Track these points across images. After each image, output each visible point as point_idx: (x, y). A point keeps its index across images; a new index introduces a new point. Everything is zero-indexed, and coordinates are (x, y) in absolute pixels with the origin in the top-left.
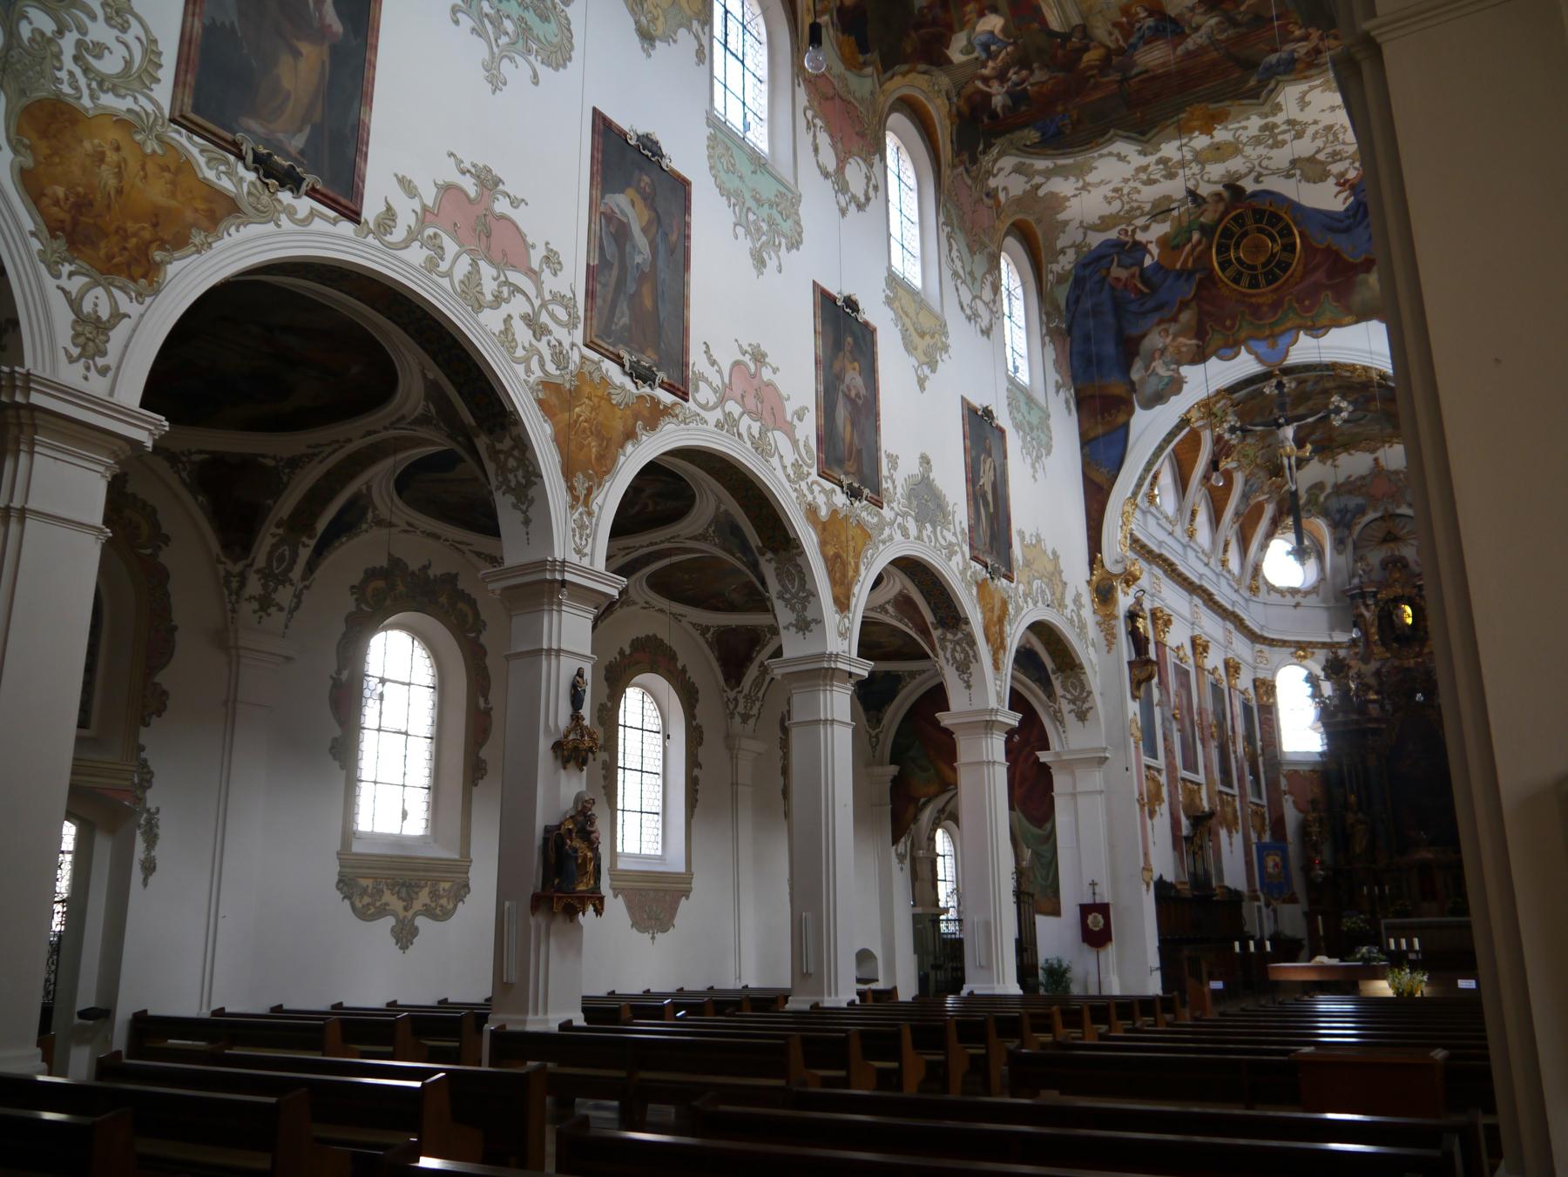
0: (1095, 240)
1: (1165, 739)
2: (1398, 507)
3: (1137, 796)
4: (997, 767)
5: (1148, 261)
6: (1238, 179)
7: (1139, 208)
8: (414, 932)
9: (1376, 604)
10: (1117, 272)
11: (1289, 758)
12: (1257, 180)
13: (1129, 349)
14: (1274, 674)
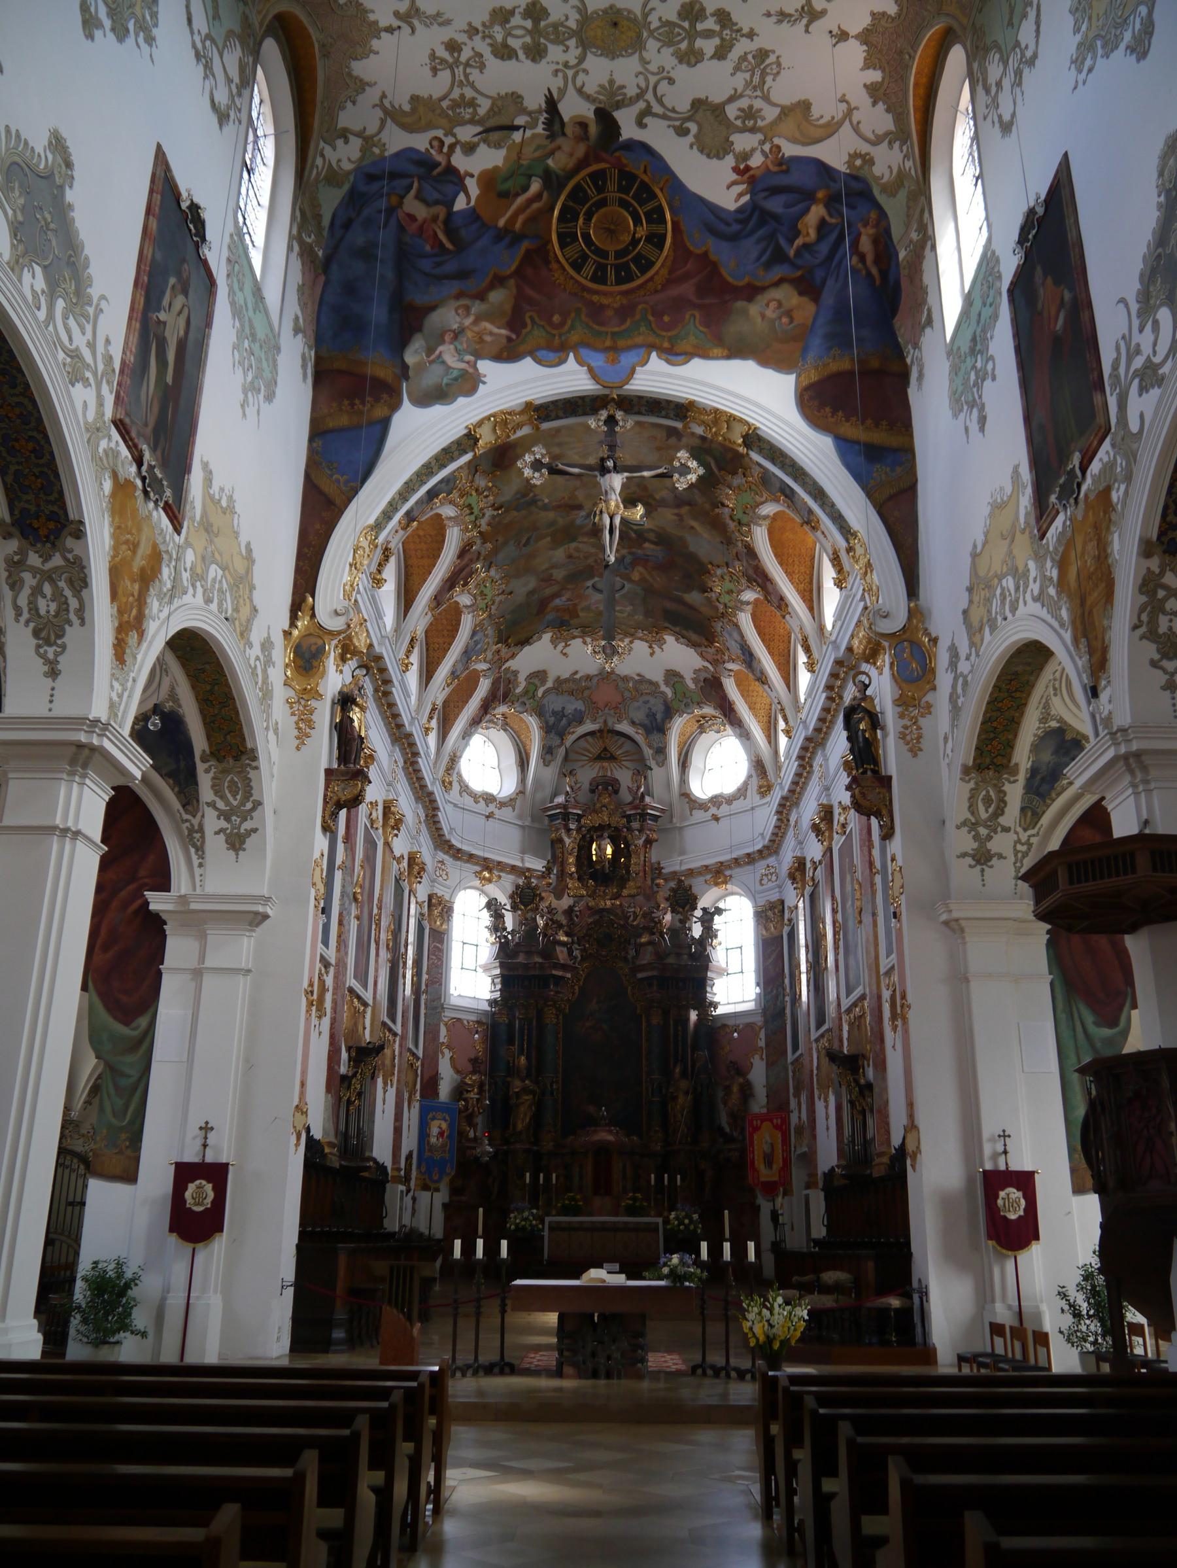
0: (396, 140)
1: (341, 923)
2: (619, 722)
3: (305, 984)
4: (80, 845)
5: (460, 204)
6: (619, 105)
7: (472, 103)
9: (579, 830)
10: (412, 206)
11: (454, 1001)
12: (641, 124)
13: (408, 321)
14: (454, 891)
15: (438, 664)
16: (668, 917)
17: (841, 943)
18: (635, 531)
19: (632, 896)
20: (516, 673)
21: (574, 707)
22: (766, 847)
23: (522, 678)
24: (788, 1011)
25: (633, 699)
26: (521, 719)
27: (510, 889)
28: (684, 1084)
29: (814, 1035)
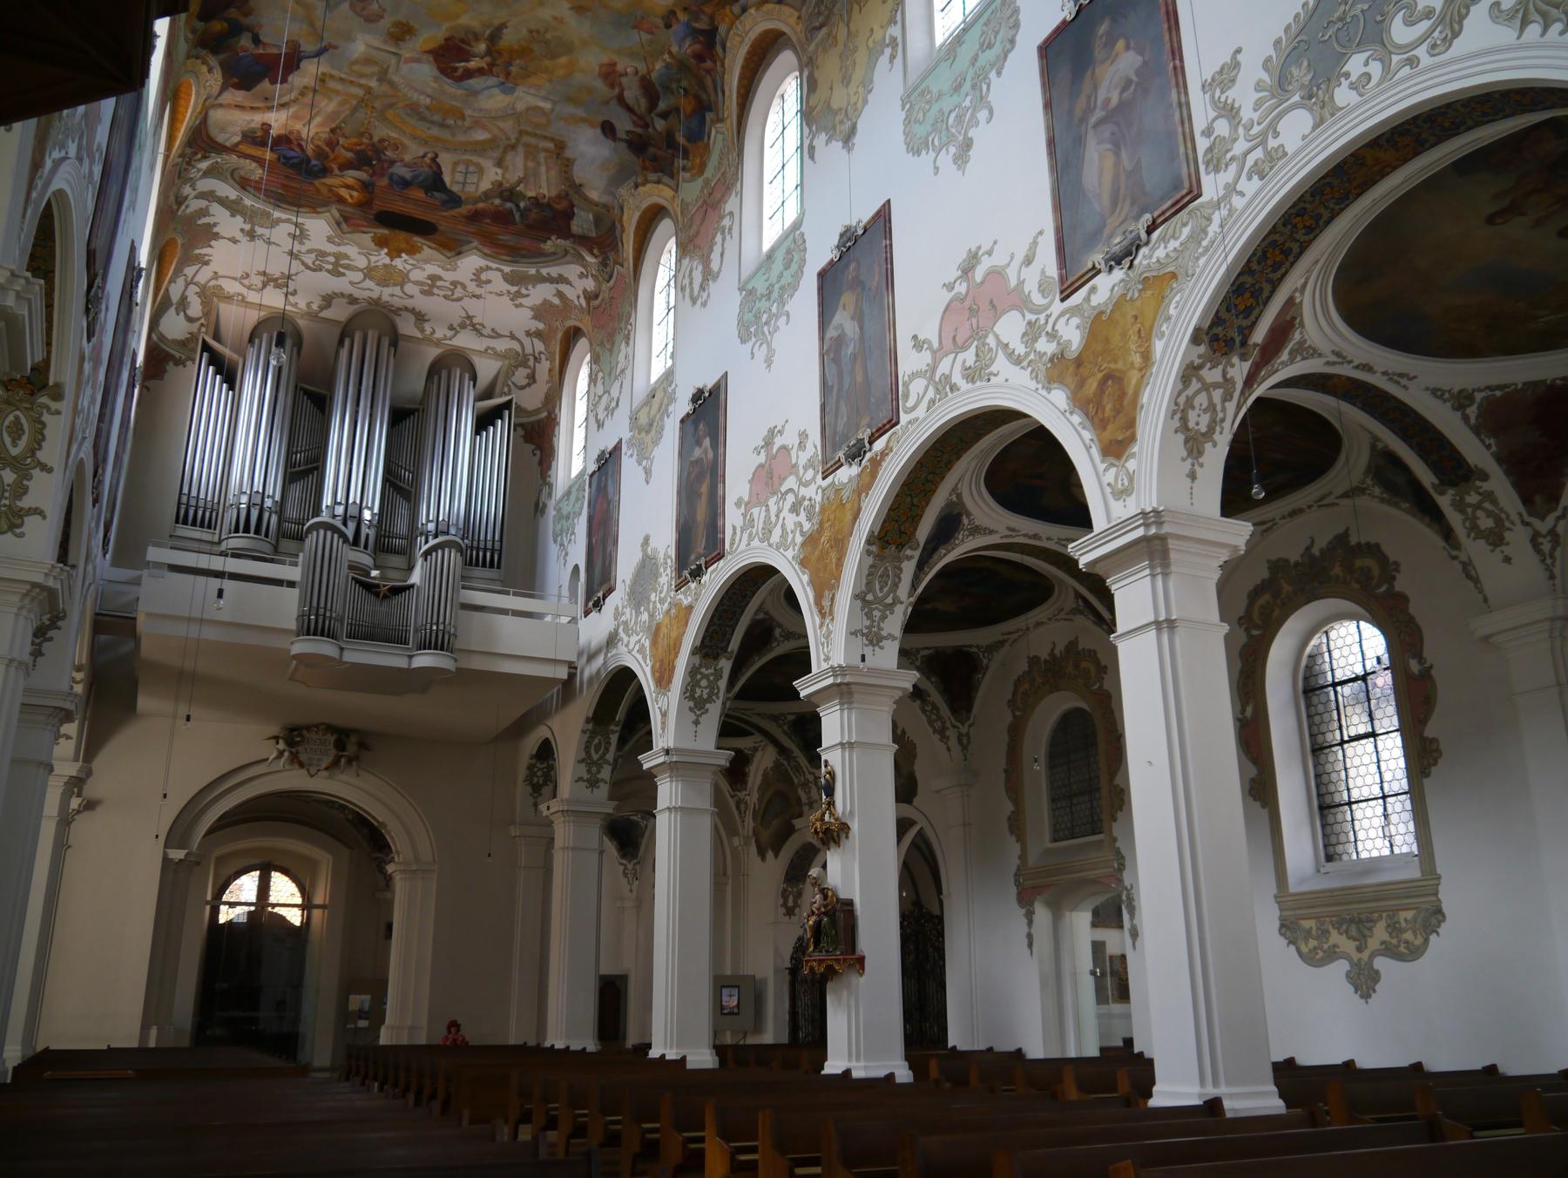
8: (1375, 977)
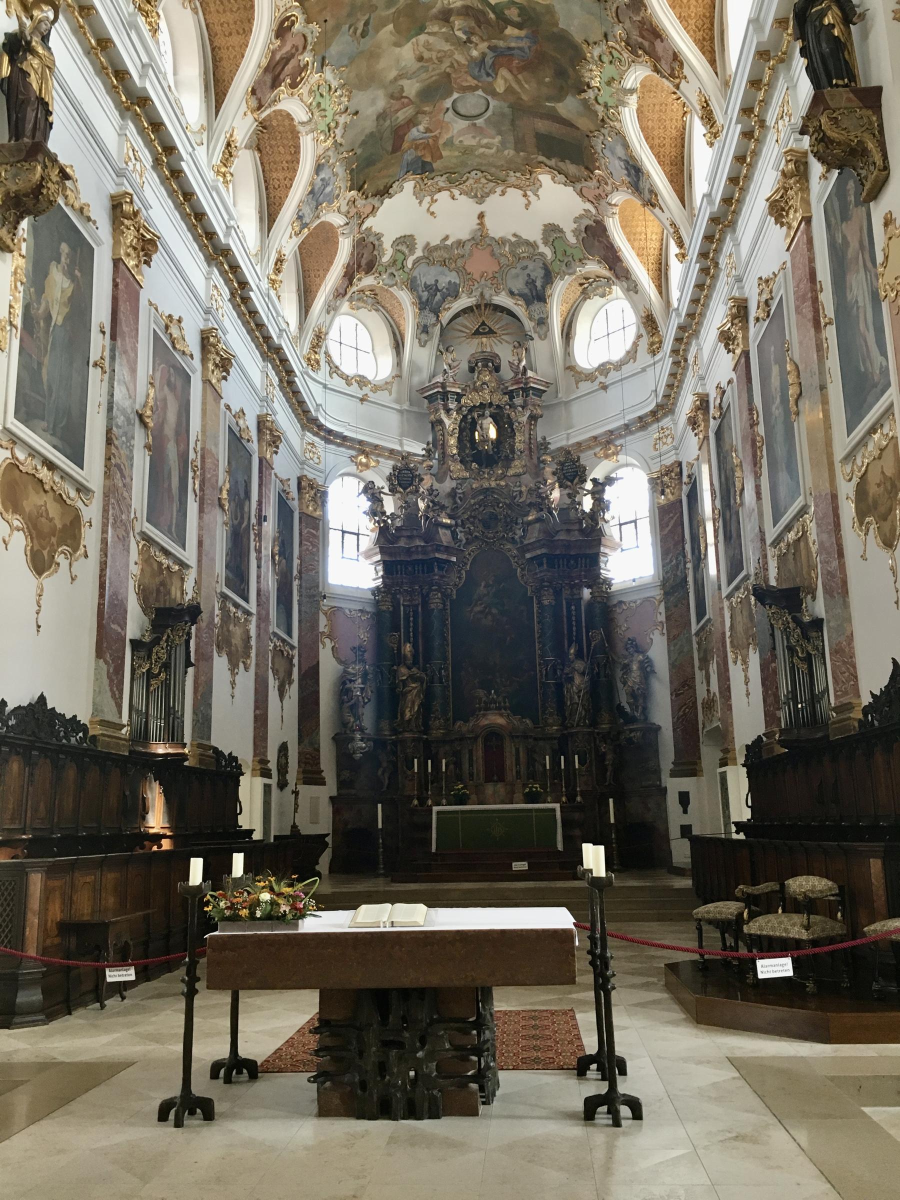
2: (497, 294)
9: (459, 411)
15: (281, 205)
16: (556, 494)
17: (764, 461)
18: (493, 8)
19: (518, 475)
20: (379, 236)
21: (448, 280)
22: (659, 406)
23: (387, 243)
24: (690, 579)
25: (511, 266)
26: (392, 295)
27: (388, 471)
28: (579, 665)
29: (725, 592)
